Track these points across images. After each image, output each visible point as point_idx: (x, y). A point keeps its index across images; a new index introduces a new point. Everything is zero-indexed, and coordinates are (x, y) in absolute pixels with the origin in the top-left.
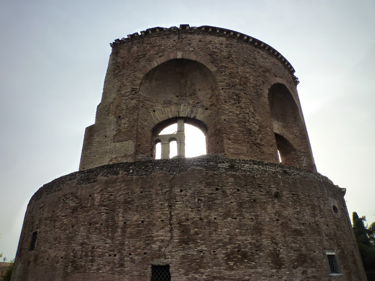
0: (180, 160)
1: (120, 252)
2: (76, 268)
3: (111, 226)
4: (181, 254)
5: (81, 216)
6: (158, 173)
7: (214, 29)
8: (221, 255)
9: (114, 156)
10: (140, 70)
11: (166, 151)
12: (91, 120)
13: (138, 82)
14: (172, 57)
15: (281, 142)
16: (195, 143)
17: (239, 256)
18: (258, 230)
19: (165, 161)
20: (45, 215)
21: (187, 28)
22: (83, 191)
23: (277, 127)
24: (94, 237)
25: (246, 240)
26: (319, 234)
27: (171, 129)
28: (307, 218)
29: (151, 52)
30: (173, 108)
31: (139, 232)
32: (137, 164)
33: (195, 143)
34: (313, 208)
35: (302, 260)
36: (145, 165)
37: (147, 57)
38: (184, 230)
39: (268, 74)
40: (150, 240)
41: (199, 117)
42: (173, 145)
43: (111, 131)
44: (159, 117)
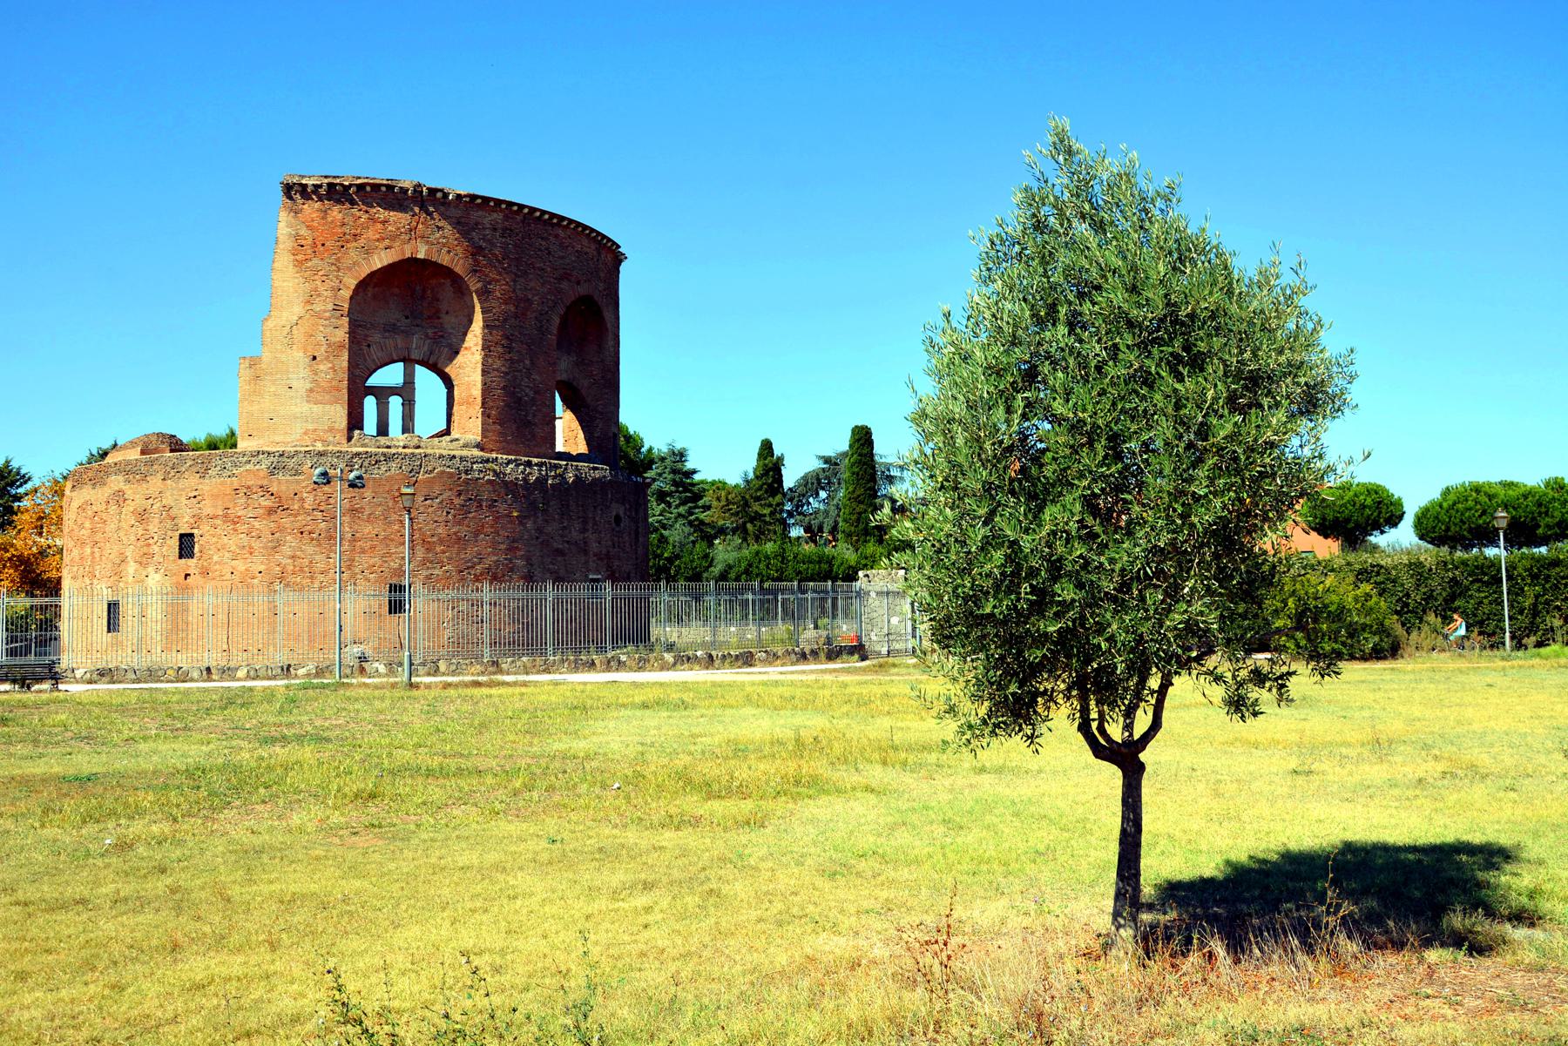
1: (349, 567)
2: (287, 585)
4: (425, 573)
5: (286, 521)
7: (486, 200)
9: (311, 427)
10: (349, 269)
13: (346, 294)
14: (408, 255)
20: (208, 510)
21: (439, 195)
22: (282, 484)
24: (310, 549)
26: (586, 552)
27: (390, 375)
28: (575, 535)
29: (371, 234)
30: (399, 340)
31: (373, 547)
34: (585, 522)
37: (362, 242)
39: (565, 285)
42: (395, 403)
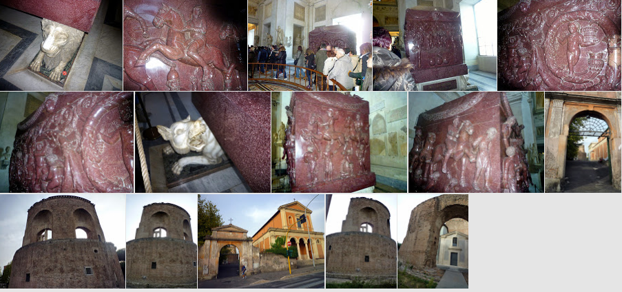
0: (160, 237)
3: (143, 253)
6: (154, 241)
8: (168, 261)
11: (156, 235)
12: (138, 227)
15: (185, 234)
16: (164, 234)
17: (173, 261)
18: (177, 255)
19: (156, 238)
22: (136, 244)
23: (184, 231)
25: (174, 257)
27: (158, 230)
32: (150, 238)
33: (164, 234)
35: (188, 263)
36: (151, 239)
38: (160, 254)
40: (152, 256)
41: (165, 227)
43: (143, 230)
44: (155, 227)
